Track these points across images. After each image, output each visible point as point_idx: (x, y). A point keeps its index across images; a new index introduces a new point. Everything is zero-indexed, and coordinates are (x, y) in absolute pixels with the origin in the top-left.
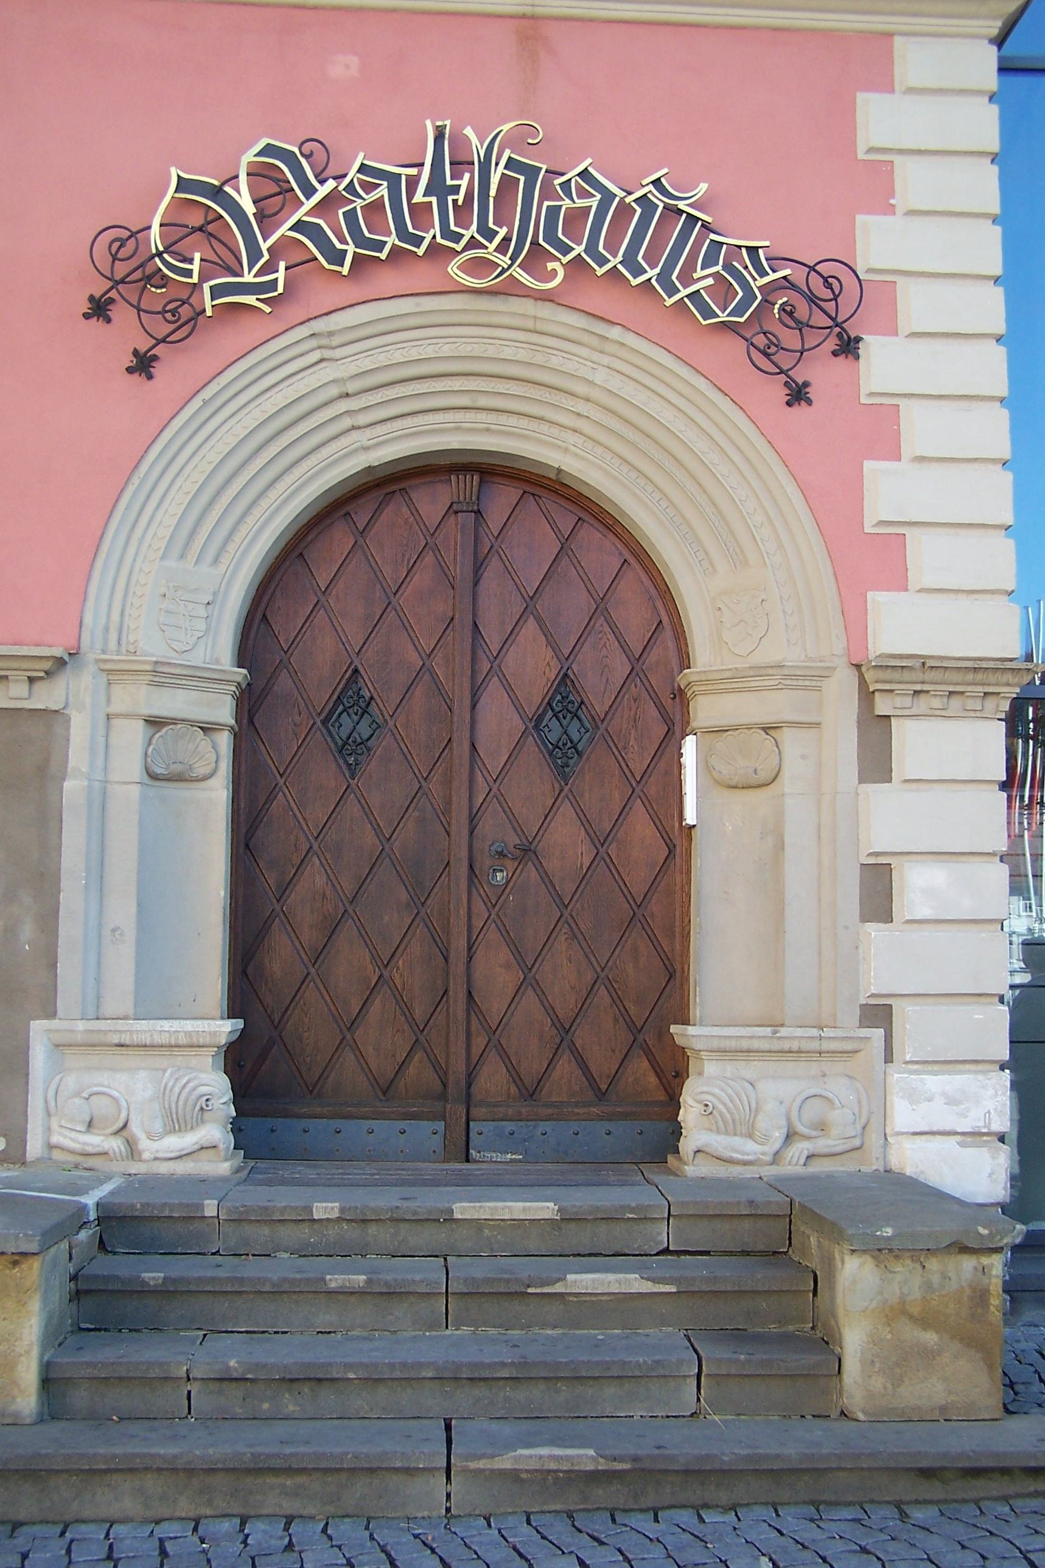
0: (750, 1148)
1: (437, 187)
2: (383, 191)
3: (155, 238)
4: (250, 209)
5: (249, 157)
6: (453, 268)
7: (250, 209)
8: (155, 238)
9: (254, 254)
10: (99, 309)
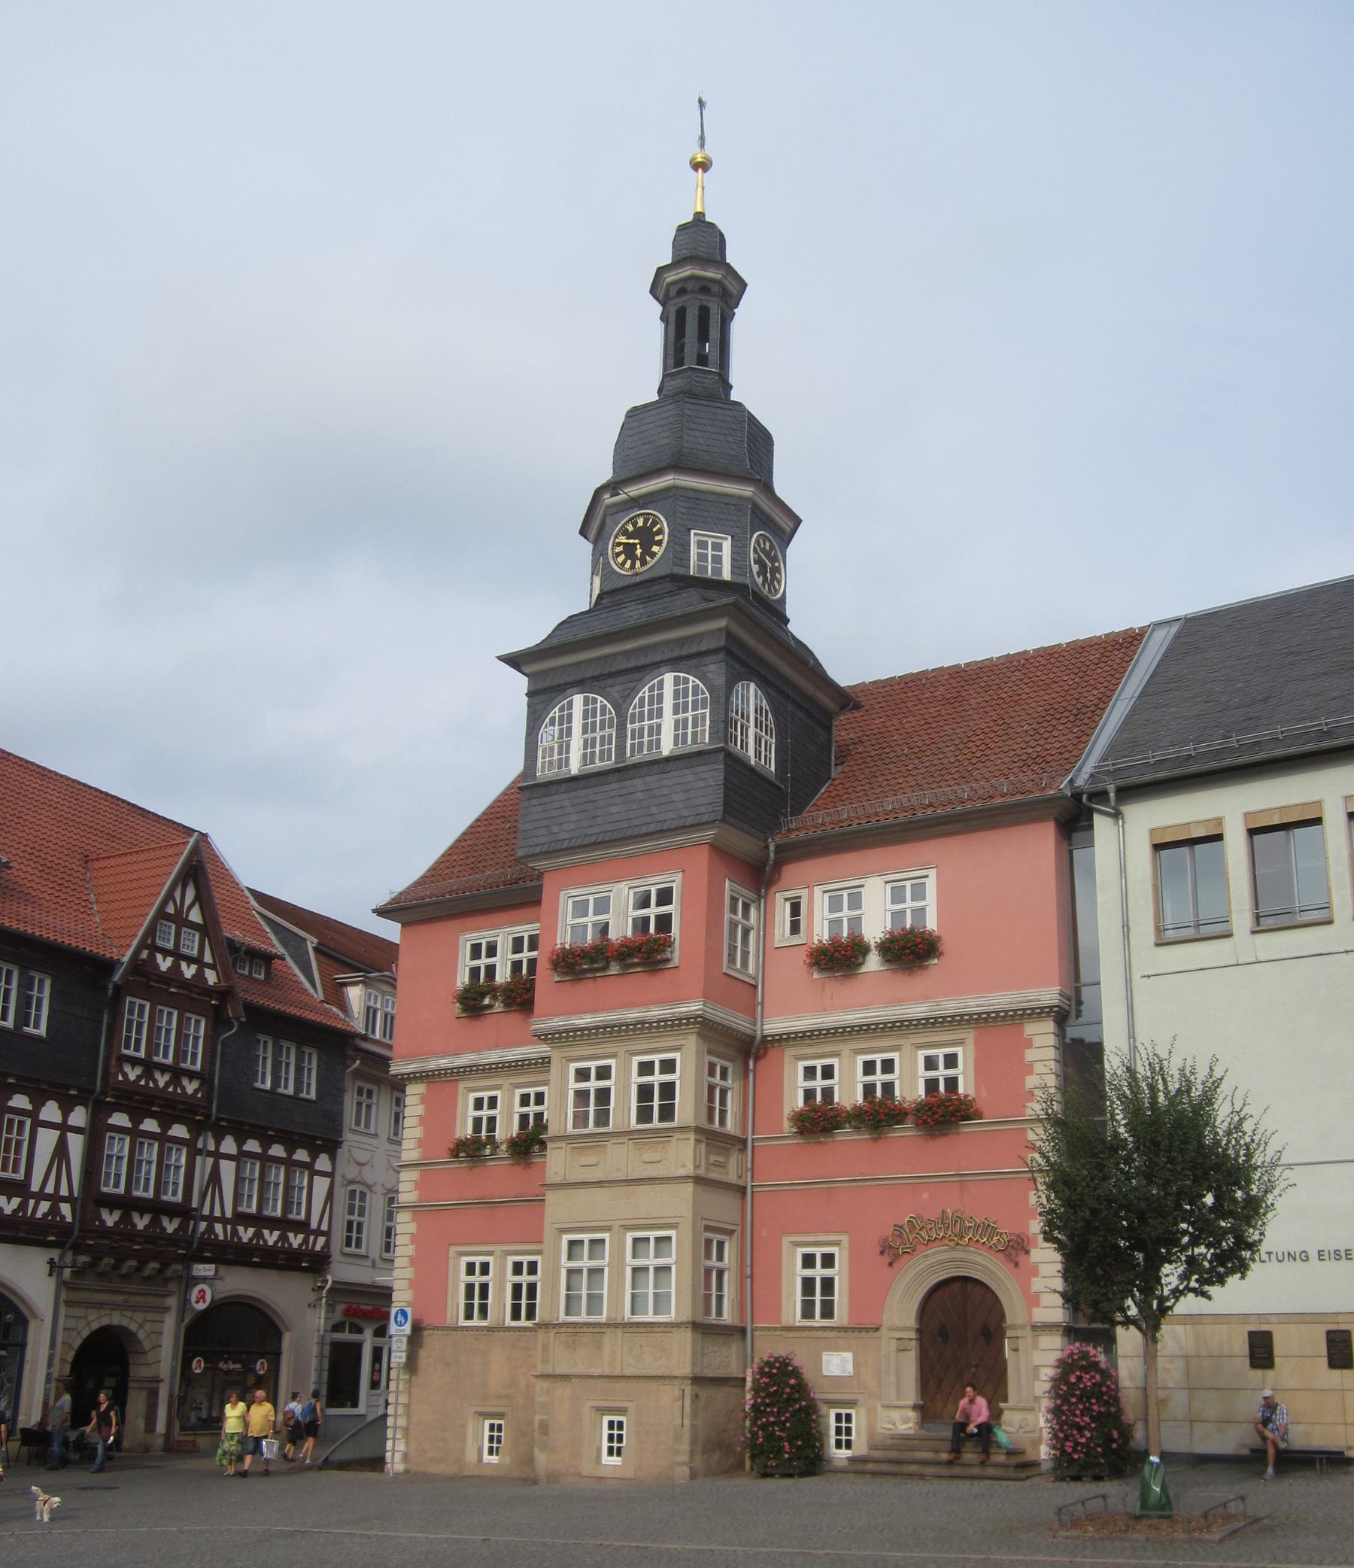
5: (907, 1219)
9: (909, 1240)
10: (882, 1253)
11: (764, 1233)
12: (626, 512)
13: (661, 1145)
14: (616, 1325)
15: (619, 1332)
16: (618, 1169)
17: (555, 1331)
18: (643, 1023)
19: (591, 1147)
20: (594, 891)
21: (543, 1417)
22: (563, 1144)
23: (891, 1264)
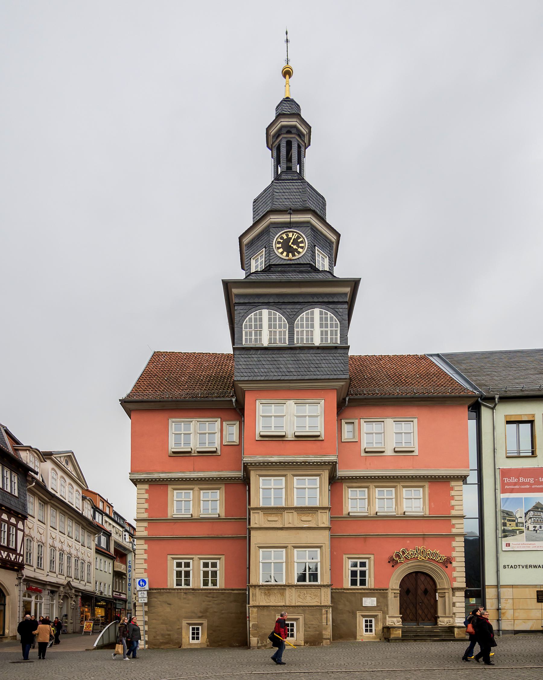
0: (444, 624)
1: (417, 552)
2: (412, 552)
3: (394, 557)
4: (401, 554)
5: (401, 550)
6: (418, 558)
7: (401, 554)
8: (394, 557)
9: (402, 558)
10: (389, 562)
11: (335, 554)
12: (287, 228)
13: (311, 514)
14: (288, 586)
15: (294, 589)
16: (290, 523)
17: (259, 588)
18: (305, 462)
19: (273, 513)
20: (275, 402)
21: (254, 623)
22: (260, 511)
23: (393, 566)
